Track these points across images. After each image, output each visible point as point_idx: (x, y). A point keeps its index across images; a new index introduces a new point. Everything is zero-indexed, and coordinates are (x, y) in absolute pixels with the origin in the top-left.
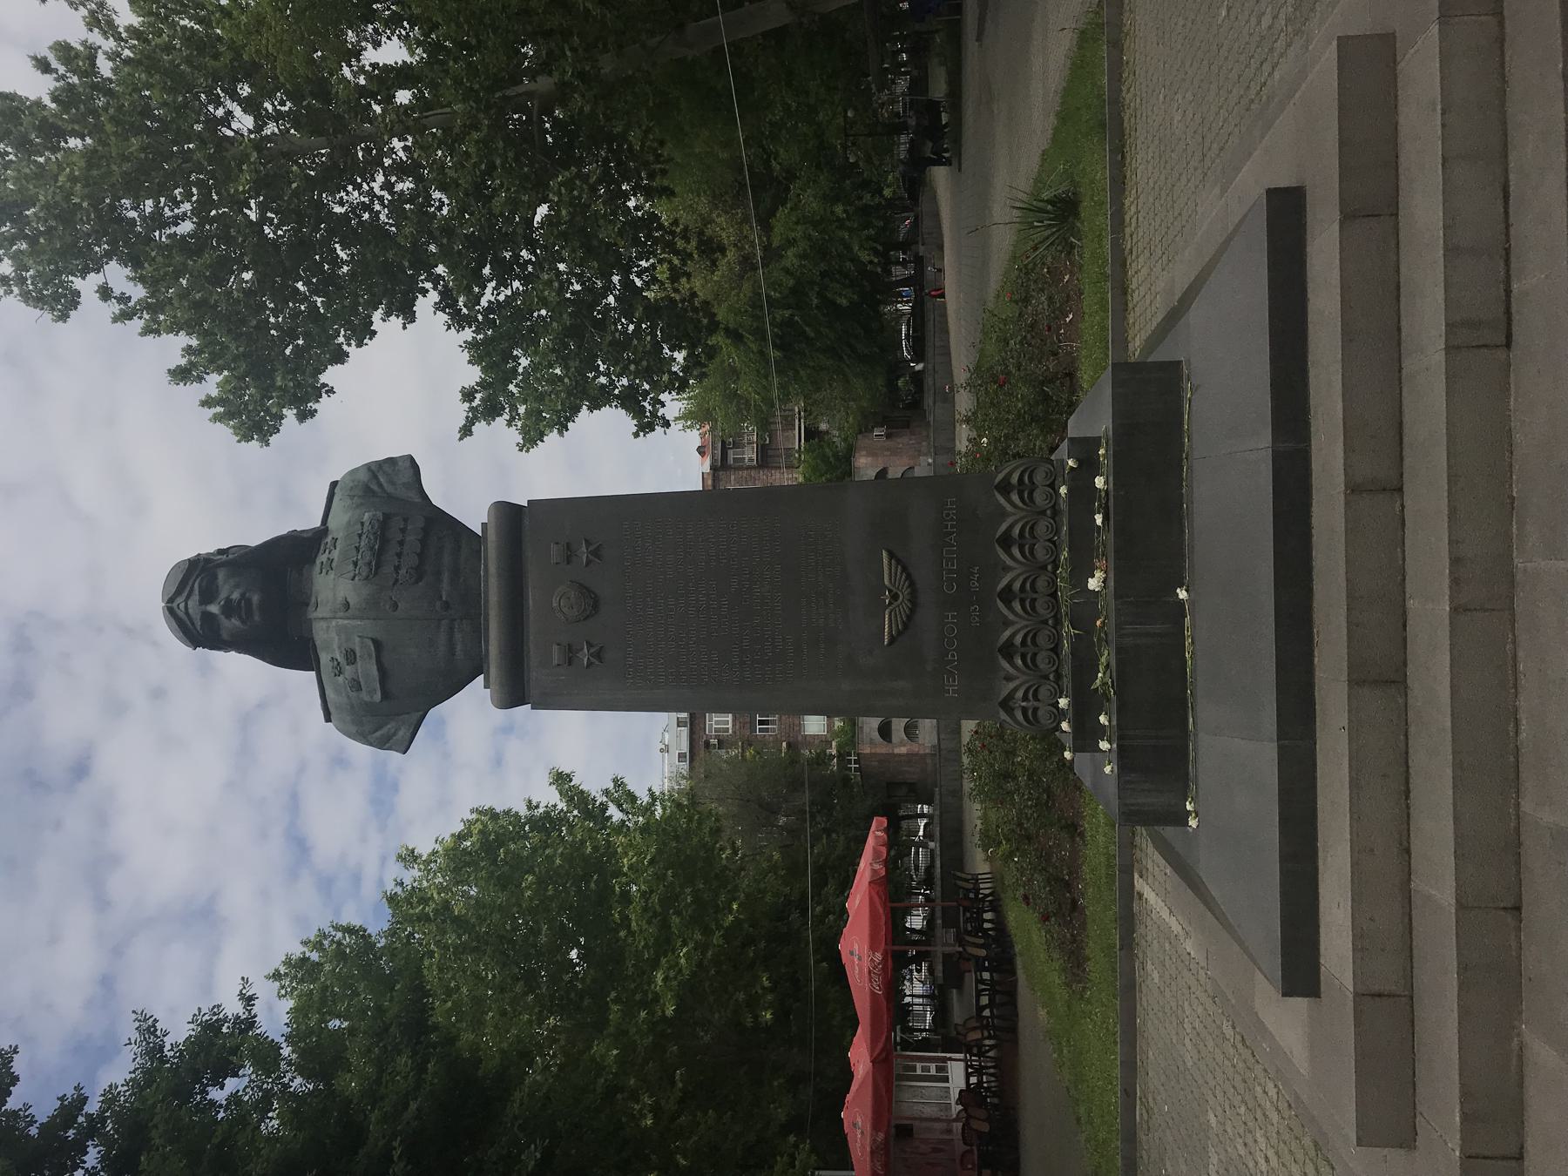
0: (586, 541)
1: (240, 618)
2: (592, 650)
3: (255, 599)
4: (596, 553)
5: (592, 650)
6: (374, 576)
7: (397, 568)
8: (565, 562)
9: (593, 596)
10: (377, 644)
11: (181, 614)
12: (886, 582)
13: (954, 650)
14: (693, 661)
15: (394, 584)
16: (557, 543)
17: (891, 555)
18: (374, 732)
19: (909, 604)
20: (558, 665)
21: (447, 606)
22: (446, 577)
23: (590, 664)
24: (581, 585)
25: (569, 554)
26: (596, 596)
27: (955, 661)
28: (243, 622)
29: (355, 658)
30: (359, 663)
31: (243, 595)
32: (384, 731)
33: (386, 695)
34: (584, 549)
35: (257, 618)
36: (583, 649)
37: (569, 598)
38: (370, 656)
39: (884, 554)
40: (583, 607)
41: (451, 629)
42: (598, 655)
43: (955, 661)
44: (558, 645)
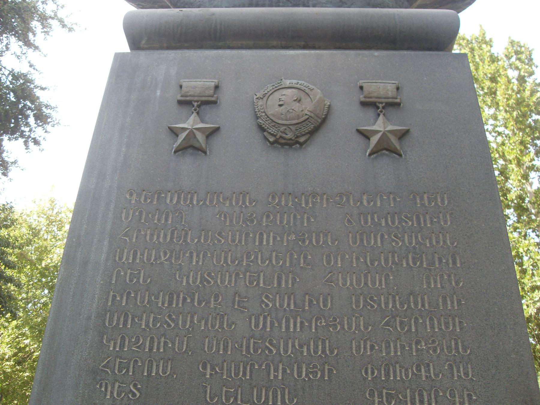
0: (407, 132)
2: (200, 137)
5: (200, 137)
8: (363, 99)
9: (302, 140)
14: (155, 319)
16: (398, 89)
20: (181, 87)
23: (174, 132)
24: (324, 120)
26: (301, 144)
34: (390, 128)
36: (202, 121)
37: (299, 101)
40: (280, 122)
44: (217, 87)
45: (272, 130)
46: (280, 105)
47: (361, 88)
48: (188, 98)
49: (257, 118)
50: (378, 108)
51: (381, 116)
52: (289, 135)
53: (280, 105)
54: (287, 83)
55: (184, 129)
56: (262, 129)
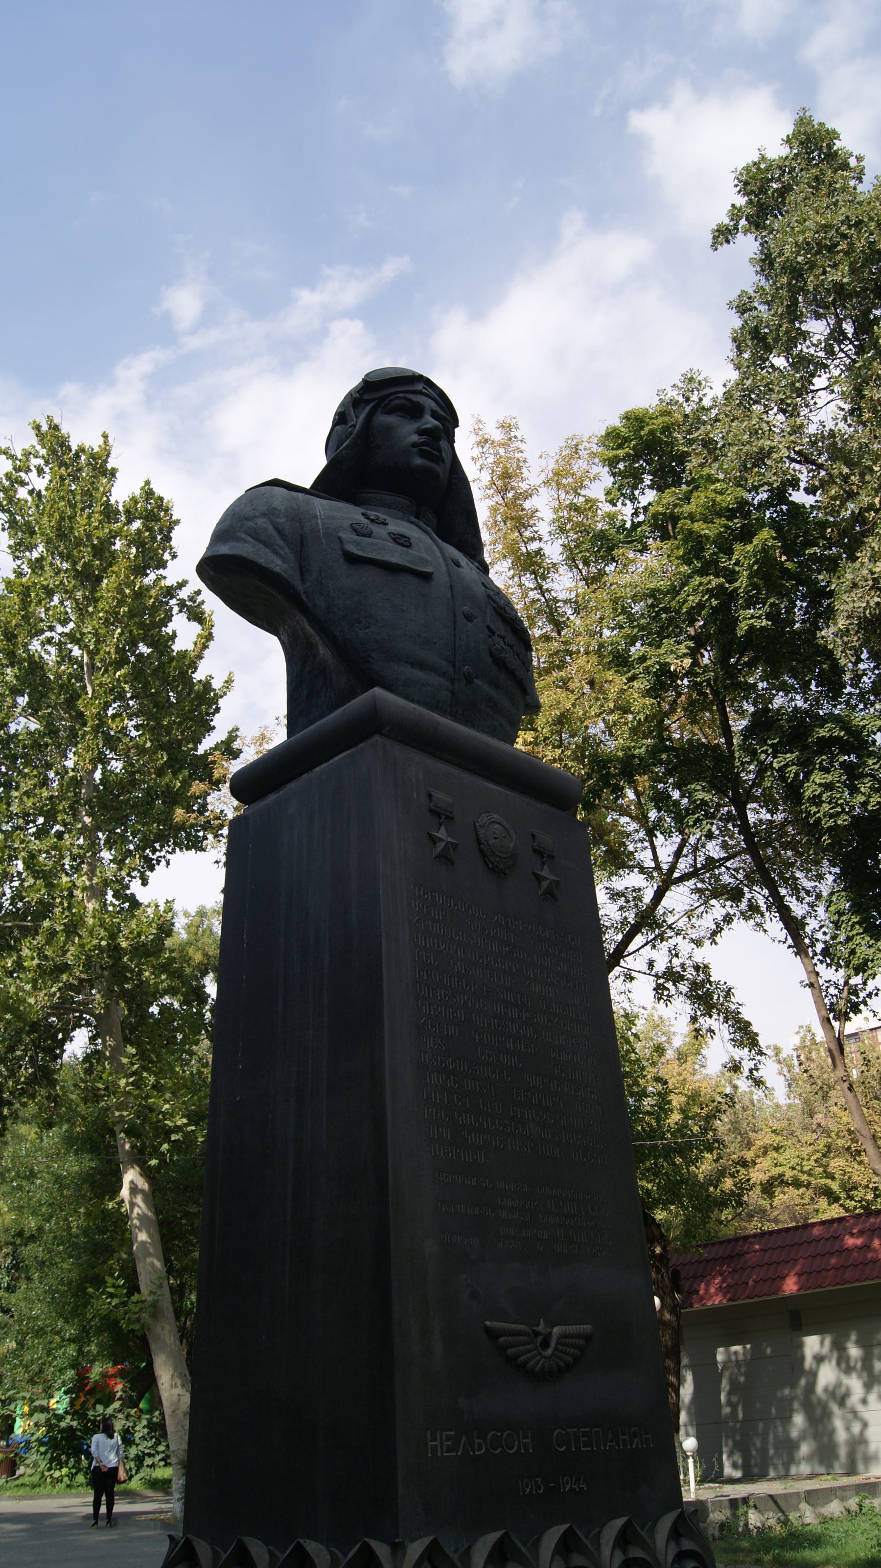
1: (423, 444)
3: (438, 469)
4: (550, 895)
6: (495, 609)
7: (503, 638)
10: (426, 577)
11: (420, 386)
12: (556, 1330)
13: (487, 1449)
15: (488, 627)
17: (588, 1338)
18: (279, 531)
19: (539, 1366)
21: (468, 679)
22: (493, 693)
23: (434, 840)
25: (543, 855)
27: (474, 1452)
28: (414, 445)
29: (402, 545)
30: (391, 545)
31: (443, 461)
32: (281, 543)
33: (352, 559)
35: (418, 461)
38: (411, 562)
39: (587, 1328)
41: (443, 675)
42: (445, 858)
43: (474, 1452)
45: (492, 859)
46: (495, 838)
47: (533, 836)
48: (438, 810)
49: (479, 843)
50: (543, 857)
51: (546, 866)
52: (501, 866)
53: (495, 838)
54: (496, 817)
55: (441, 840)
56: (483, 854)
